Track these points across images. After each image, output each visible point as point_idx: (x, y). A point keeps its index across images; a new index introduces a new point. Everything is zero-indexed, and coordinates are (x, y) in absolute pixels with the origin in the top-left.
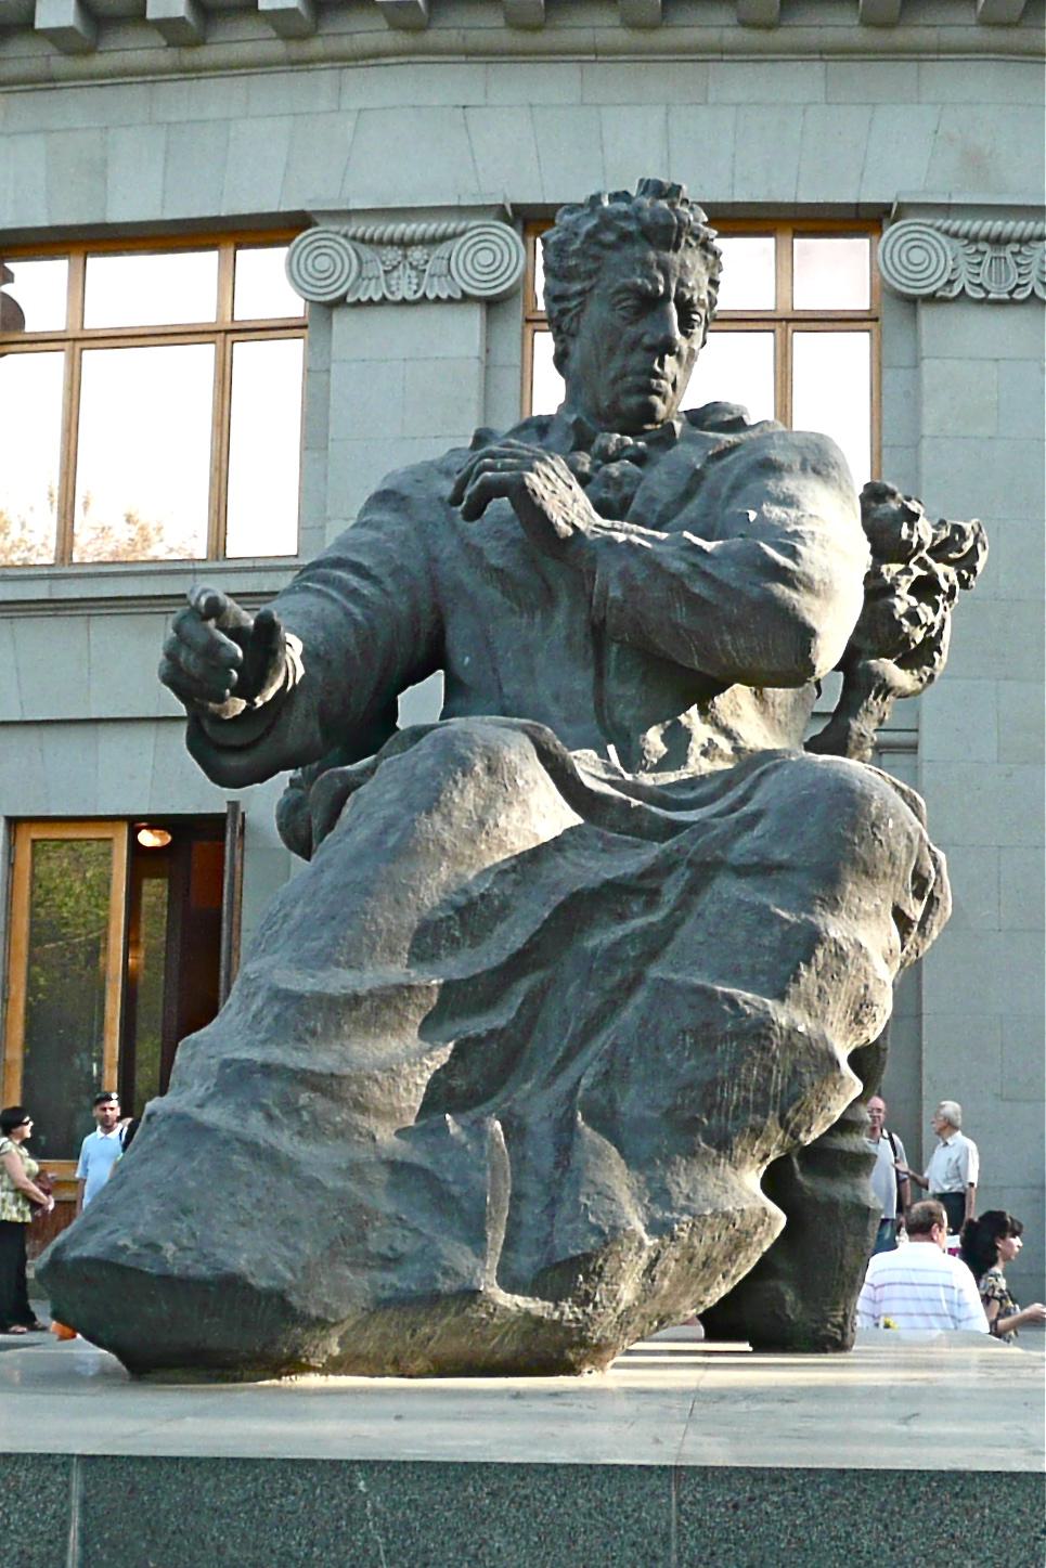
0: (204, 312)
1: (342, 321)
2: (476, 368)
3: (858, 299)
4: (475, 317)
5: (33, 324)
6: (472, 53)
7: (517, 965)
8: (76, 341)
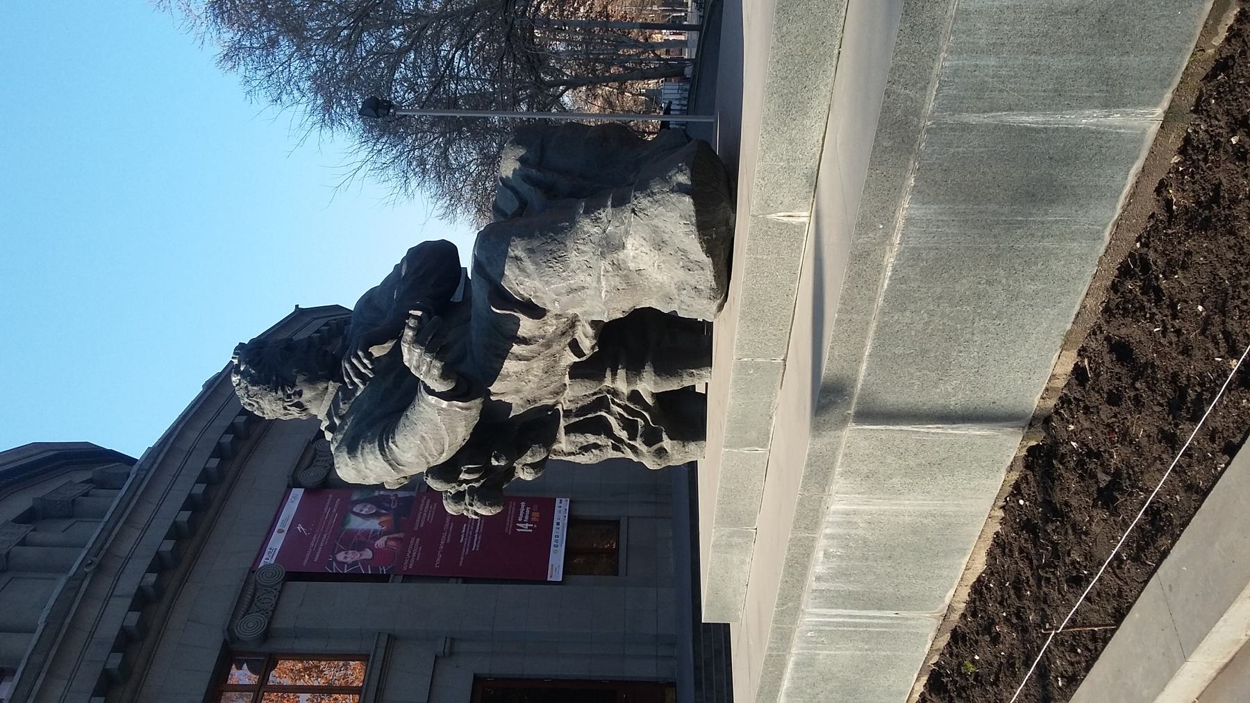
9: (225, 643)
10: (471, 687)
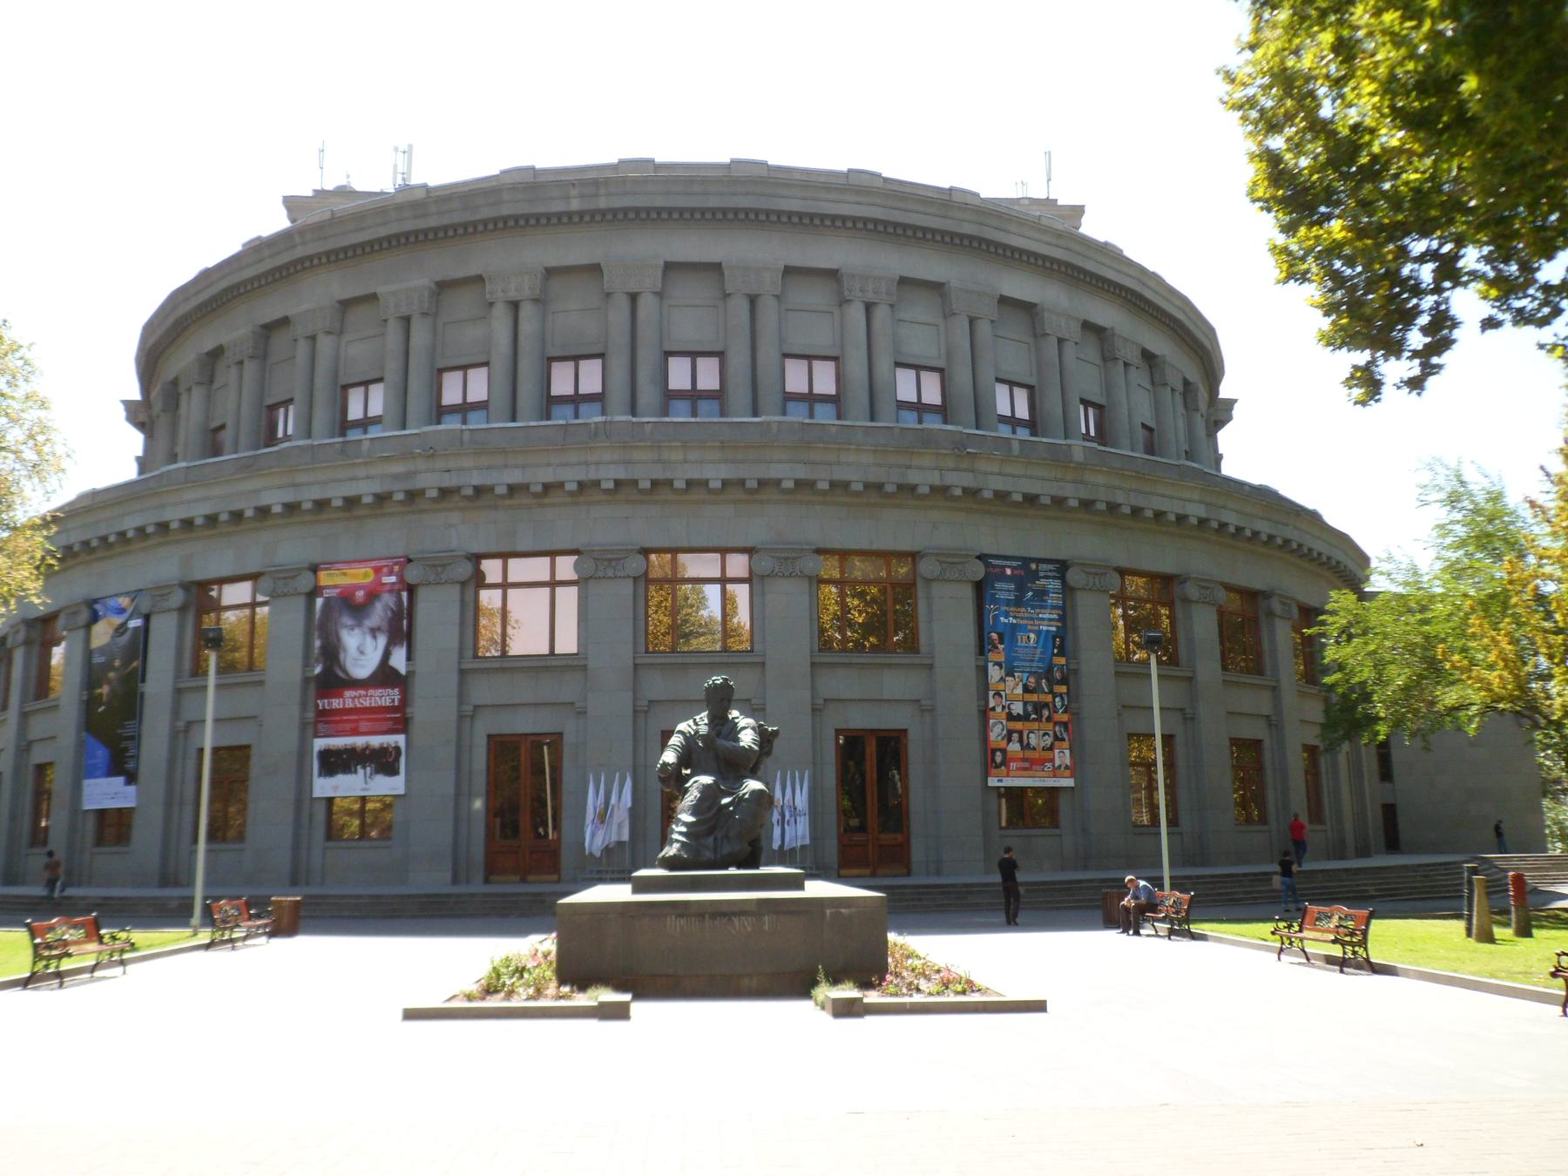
0: (547, 578)
1: (592, 583)
2: (632, 597)
3: (745, 574)
4: (629, 585)
5: (489, 580)
6: (629, 502)
7: (715, 814)
8: (505, 586)
9: (919, 552)
10: (897, 727)
